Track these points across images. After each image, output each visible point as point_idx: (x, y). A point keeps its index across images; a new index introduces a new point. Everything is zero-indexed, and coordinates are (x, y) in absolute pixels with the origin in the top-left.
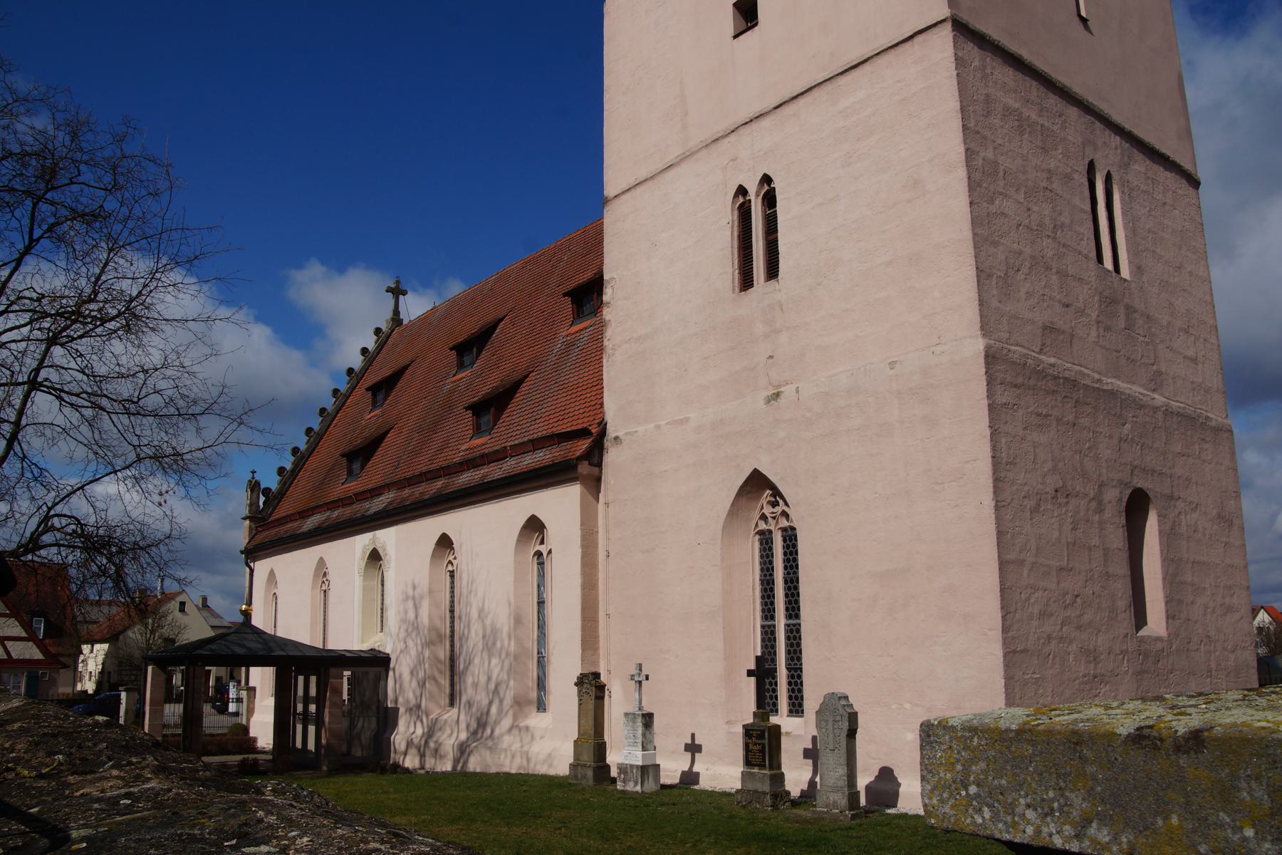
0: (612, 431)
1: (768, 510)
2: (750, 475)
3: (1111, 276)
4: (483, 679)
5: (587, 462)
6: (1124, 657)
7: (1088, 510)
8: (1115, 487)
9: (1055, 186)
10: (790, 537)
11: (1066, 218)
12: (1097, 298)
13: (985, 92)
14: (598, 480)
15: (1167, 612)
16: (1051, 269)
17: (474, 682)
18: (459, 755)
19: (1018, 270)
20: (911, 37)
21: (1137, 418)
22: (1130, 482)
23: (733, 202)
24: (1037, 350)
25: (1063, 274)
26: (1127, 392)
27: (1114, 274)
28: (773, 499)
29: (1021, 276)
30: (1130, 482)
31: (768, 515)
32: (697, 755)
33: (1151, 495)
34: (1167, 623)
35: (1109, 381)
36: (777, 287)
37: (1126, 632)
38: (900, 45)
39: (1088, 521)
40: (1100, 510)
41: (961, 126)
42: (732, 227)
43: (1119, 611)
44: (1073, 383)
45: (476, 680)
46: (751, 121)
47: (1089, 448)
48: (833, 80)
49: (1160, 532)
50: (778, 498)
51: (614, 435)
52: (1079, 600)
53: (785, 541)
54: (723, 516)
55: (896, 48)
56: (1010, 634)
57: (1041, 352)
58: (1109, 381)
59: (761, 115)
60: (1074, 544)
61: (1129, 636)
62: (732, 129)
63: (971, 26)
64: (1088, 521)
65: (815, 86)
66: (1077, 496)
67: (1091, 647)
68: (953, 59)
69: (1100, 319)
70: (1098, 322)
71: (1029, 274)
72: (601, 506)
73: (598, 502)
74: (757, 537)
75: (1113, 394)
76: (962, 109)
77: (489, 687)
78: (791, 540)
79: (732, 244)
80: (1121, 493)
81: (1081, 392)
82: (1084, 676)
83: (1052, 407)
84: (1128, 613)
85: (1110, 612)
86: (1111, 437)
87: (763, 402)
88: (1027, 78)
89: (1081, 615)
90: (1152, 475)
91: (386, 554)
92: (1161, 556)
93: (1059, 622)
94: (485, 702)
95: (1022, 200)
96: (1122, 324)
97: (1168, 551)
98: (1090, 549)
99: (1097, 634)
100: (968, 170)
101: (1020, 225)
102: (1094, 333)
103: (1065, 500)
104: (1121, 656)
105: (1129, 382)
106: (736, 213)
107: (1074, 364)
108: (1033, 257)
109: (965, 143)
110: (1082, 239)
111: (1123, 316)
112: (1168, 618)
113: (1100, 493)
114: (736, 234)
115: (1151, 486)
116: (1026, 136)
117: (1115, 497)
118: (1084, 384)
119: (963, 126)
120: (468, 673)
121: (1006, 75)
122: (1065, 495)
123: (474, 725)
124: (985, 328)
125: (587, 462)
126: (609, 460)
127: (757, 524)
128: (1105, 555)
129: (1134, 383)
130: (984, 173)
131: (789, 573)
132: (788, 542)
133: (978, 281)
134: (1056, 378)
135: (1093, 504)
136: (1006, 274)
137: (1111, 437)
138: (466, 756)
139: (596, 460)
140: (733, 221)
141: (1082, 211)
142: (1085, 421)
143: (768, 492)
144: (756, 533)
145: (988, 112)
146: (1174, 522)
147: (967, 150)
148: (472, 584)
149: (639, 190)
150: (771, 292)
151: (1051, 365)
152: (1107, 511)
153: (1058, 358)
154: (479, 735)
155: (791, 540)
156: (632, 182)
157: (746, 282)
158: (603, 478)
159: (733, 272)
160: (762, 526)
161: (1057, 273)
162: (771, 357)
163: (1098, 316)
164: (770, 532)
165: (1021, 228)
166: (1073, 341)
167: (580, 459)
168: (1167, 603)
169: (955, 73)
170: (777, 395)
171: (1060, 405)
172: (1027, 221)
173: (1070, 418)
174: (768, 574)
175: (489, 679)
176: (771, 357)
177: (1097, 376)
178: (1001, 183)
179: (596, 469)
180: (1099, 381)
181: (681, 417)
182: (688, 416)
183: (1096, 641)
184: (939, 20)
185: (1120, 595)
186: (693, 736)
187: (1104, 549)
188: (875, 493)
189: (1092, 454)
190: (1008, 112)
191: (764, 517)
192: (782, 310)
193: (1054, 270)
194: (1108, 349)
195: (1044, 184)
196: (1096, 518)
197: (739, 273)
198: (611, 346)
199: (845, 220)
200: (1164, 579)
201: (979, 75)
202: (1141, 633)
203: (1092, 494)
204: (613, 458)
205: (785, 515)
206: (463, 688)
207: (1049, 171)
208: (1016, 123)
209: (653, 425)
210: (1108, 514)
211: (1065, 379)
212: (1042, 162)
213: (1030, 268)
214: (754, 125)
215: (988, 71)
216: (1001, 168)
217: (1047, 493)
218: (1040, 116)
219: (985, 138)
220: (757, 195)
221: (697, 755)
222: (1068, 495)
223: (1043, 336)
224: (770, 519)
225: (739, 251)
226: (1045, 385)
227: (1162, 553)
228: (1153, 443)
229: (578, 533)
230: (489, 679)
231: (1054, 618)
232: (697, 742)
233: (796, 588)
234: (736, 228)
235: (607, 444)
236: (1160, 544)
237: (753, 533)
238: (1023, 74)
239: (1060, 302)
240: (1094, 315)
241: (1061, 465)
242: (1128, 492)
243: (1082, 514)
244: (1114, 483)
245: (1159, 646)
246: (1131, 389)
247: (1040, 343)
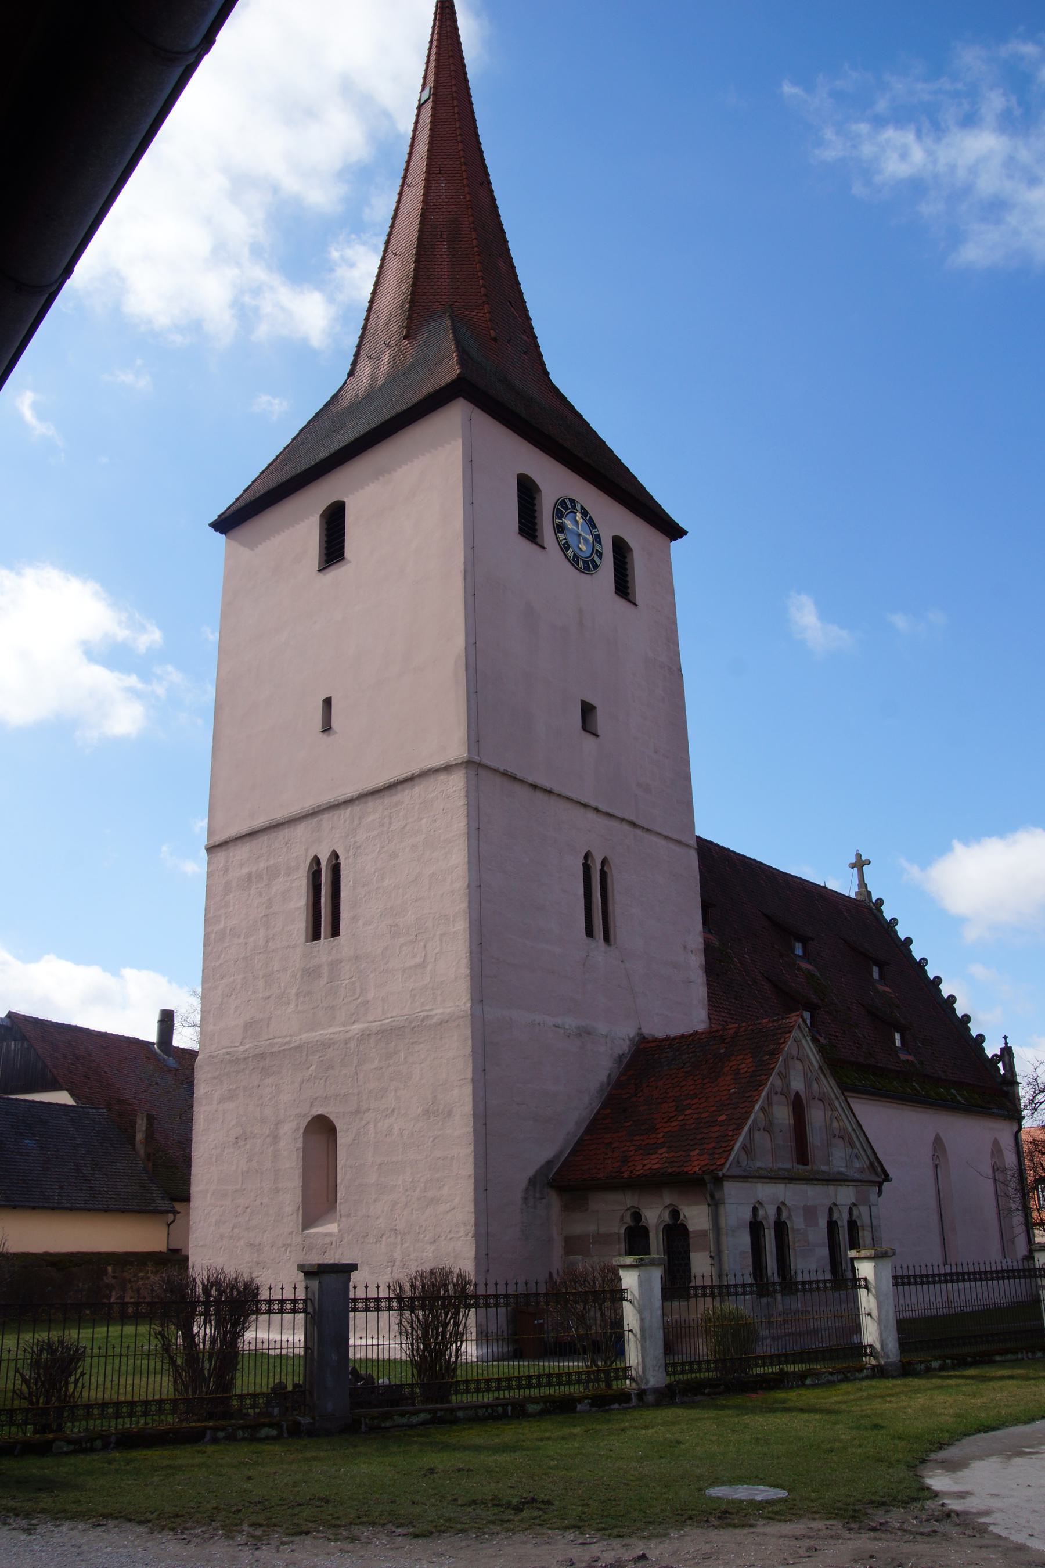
6: (286, 1250)
7: (263, 1145)
30: (308, 1113)
37: (291, 1230)
39: (262, 1153)
47: (270, 1099)
52: (249, 1210)
60: (248, 1172)
61: (294, 1233)
64: (262, 1153)
66: (254, 1137)
67: (257, 1242)
75: (299, 1048)
82: (248, 1262)
84: (295, 1215)
103: (243, 1143)
104: (283, 1249)
135: (269, 1140)
185: (288, 1202)
210: (282, 1144)
244: (292, 1118)
245: (328, 1240)
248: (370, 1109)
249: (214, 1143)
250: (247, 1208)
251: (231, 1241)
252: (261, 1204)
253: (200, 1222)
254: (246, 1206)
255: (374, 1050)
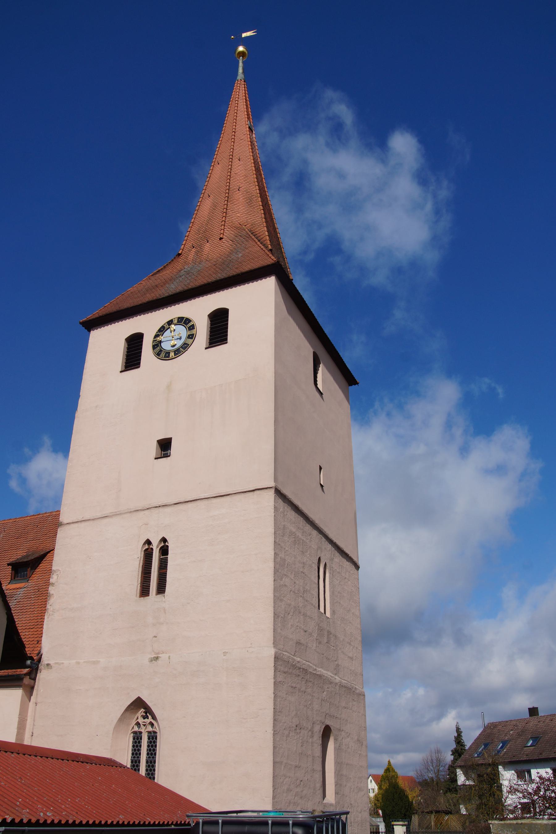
0: (45, 660)
1: (141, 720)
2: (135, 700)
3: (323, 616)
5: (29, 677)
8: (318, 724)
9: (305, 571)
10: (153, 738)
11: (308, 588)
12: (317, 627)
13: (283, 524)
14: (32, 688)
15: (335, 790)
16: (301, 613)
19: (289, 614)
20: (253, 491)
21: (329, 689)
22: (324, 722)
23: (142, 547)
24: (293, 654)
25: (305, 615)
26: (326, 675)
27: (324, 614)
28: (144, 714)
29: (290, 617)
30: (324, 722)
31: (141, 723)
33: (332, 728)
34: (335, 796)
35: (319, 669)
36: (164, 600)
38: (247, 493)
40: (312, 737)
41: (274, 541)
42: (140, 561)
43: (317, 789)
44: (305, 671)
46: (160, 507)
47: (310, 704)
48: (209, 499)
49: (335, 748)
50: (148, 714)
51: (46, 662)
53: (149, 738)
54: (115, 721)
55: (245, 493)
56: (275, 800)
57: (294, 656)
58: (319, 669)
59: (166, 505)
61: (320, 802)
62: (148, 508)
63: (282, 492)
65: (199, 499)
68: (273, 508)
69: (317, 638)
70: (317, 640)
71: (292, 616)
72: (31, 704)
73: (30, 701)
74: (132, 735)
75: (320, 676)
76: (275, 533)
78: (153, 739)
79: (139, 570)
80: (321, 727)
81: (309, 675)
83: (297, 684)
85: (313, 790)
86: (318, 698)
87: (148, 660)
88: (299, 516)
89: (302, 791)
90: (333, 718)
92: (334, 761)
93: (294, 794)
95: (293, 578)
96: (325, 640)
97: (337, 758)
98: (307, 756)
99: (308, 801)
100: (274, 564)
101: (291, 591)
102: (315, 645)
105: (326, 670)
106: (143, 553)
107: (307, 661)
108: (295, 607)
109: (274, 550)
110: (313, 598)
111: (326, 636)
112: (335, 794)
113: (313, 727)
114: (141, 564)
115: (332, 724)
116: (296, 546)
117: (318, 729)
118: (310, 672)
119: (275, 541)
121: (292, 514)
122: (299, 728)
124: (275, 644)
125: (29, 677)
126: (41, 676)
127: (133, 727)
128: (313, 760)
129: (328, 671)
130: (280, 565)
131: (149, 757)
132: (151, 740)
133: (274, 619)
134: (300, 668)
135: (310, 733)
136: (284, 616)
137: (318, 698)
139: (33, 676)
140: (141, 557)
141: (316, 584)
142: (309, 690)
143: (142, 710)
144: (132, 732)
145: (284, 534)
146: (340, 743)
147: (275, 553)
149: (83, 524)
150: (160, 602)
151: (298, 662)
152: (315, 736)
153: (301, 658)
155: (153, 739)
156: (80, 519)
157: (144, 591)
158: (36, 687)
159: (138, 585)
160: (136, 729)
161: (303, 615)
162: (155, 637)
163: (317, 636)
164: (141, 733)
165: (291, 592)
166: (307, 649)
167: (26, 674)
168: (336, 785)
169: (273, 514)
170: (157, 658)
171: (300, 682)
172: (294, 589)
173: (303, 689)
174: (136, 756)
176: (155, 637)
177: (315, 667)
178: (286, 570)
179: (32, 681)
180: (316, 670)
181: (94, 660)
182: (99, 660)
183: (307, 805)
184: (269, 487)
185: (318, 781)
187: (313, 757)
188: (209, 720)
189: (310, 708)
190: (292, 533)
191: (138, 724)
192: (165, 613)
193: (302, 614)
194: (319, 653)
195: (301, 570)
196: (311, 740)
197: (140, 586)
198: (51, 609)
199: (206, 573)
200: (335, 773)
201: (282, 515)
202: (325, 801)
203: (310, 728)
204: (43, 676)
205: (152, 724)
207: (304, 563)
208: (294, 539)
209: (74, 661)
211: (303, 669)
212: (301, 558)
213: (293, 613)
214: (161, 509)
215: (285, 513)
216: (287, 562)
217: (293, 727)
218: (303, 535)
219: (282, 547)
220: (157, 547)
222: (301, 728)
223: (296, 647)
224: (142, 725)
225: (142, 574)
226: (295, 672)
227: (335, 759)
228: (334, 701)
229: (17, 719)
231: (292, 792)
233: (153, 766)
234: (142, 562)
235: (41, 667)
236: (334, 754)
237: (130, 732)
238: (298, 514)
239: (303, 629)
240: (315, 636)
241: (299, 713)
242: (323, 727)
243: (305, 738)
246: (327, 674)
247: (294, 650)
248: (343, 730)
249: (285, 724)
250: (301, 781)
251: (294, 807)
252: (308, 779)
253: (278, 789)
254: (301, 779)
255: (343, 696)
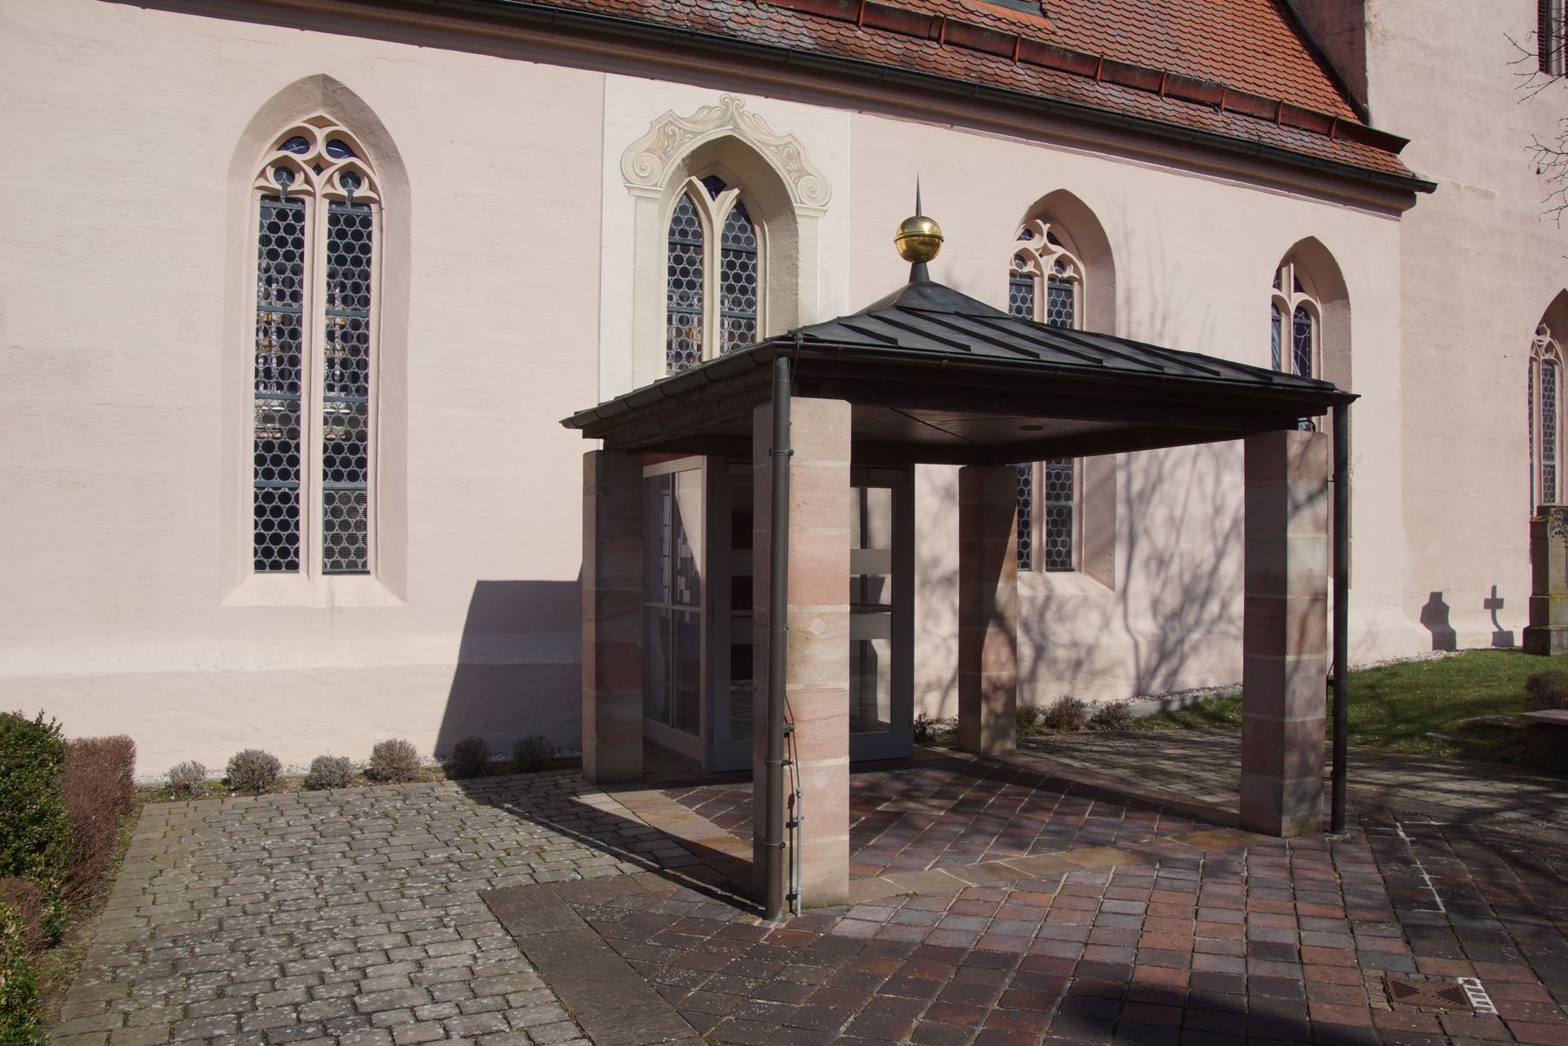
4: (1199, 510)
17: (1171, 519)
18: (1154, 662)
32: (1498, 611)
45: (1178, 512)
77: (1217, 525)
91: (803, 172)
94: (1206, 553)
120: (1156, 498)
123: (1171, 600)
138: (1174, 662)
148: (1164, 320)
154: (1190, 619)
175: (1218, 511)
186: (1494, 589)
206: (1139, 528)
221: (1498, 611)
230: (1218, 511)
232: (1498, 597)
